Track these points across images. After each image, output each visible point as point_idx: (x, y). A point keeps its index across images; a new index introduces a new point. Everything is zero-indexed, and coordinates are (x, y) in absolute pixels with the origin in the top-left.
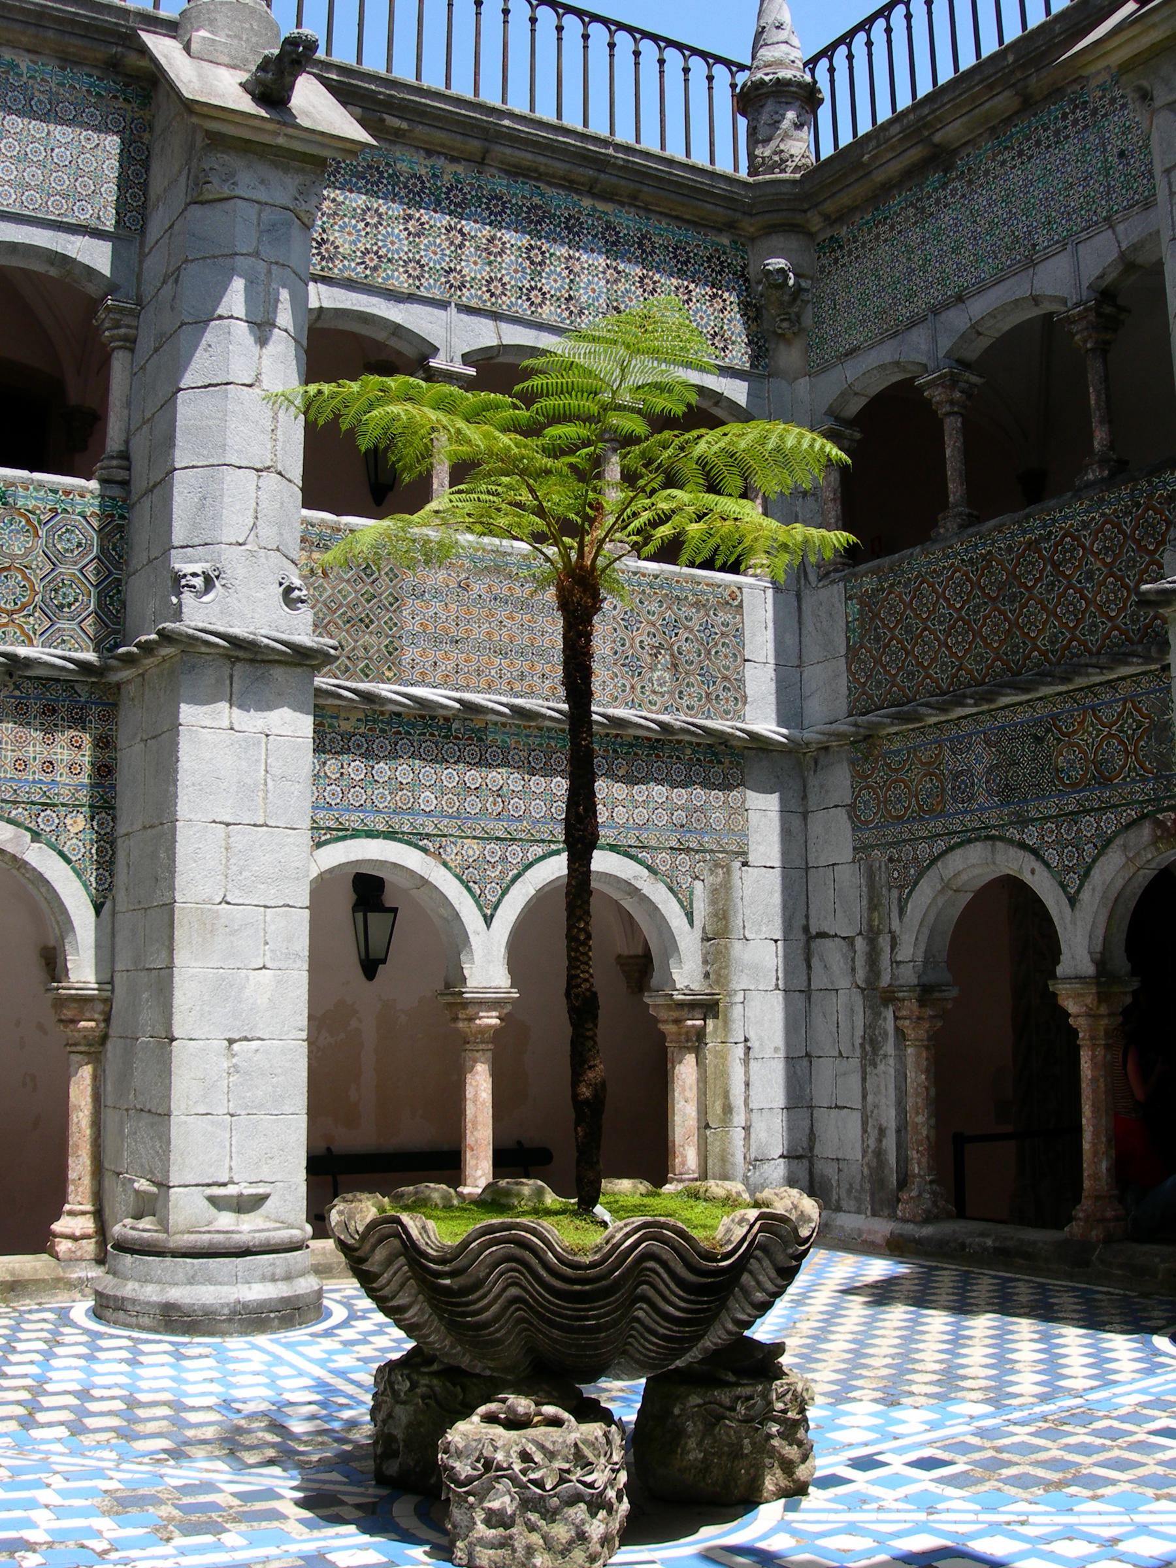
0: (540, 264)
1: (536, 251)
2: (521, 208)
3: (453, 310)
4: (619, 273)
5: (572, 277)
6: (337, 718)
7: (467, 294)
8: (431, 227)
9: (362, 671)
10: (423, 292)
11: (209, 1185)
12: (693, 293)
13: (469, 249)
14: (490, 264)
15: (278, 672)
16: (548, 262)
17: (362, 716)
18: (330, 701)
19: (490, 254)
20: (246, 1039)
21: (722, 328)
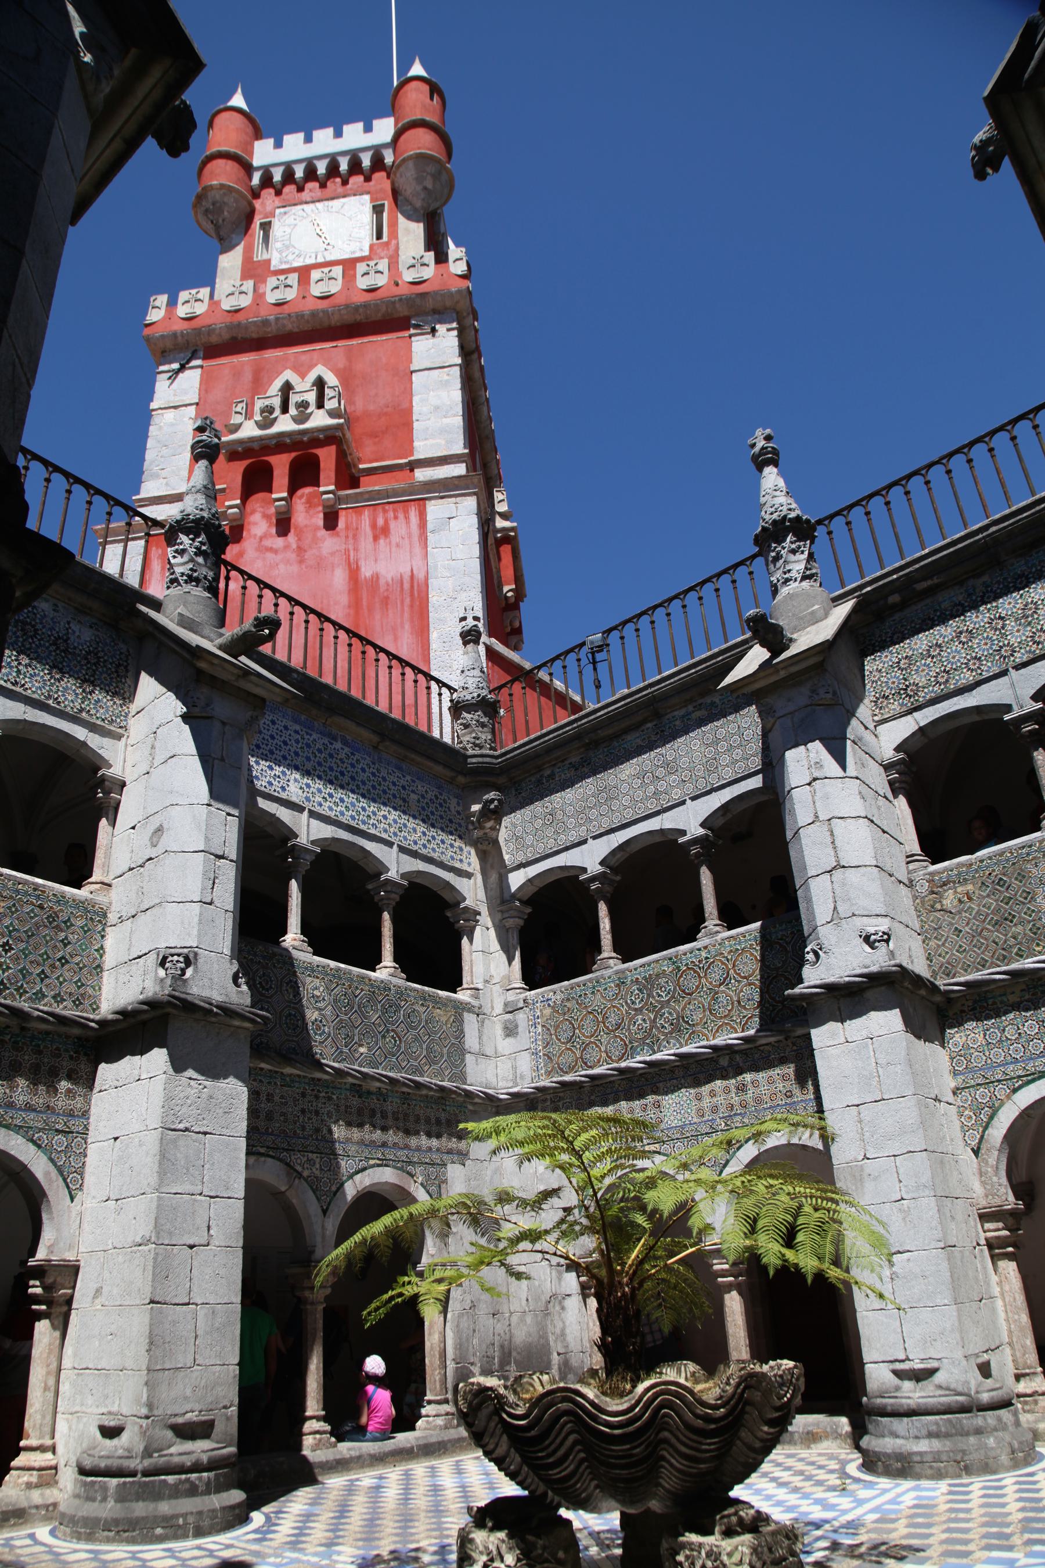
3: (1012, 672)
6: (1005, 995)
7: (1019, 655)
9: (1017, 954)
10: (986, 675)
11: (891, 1362)
13: (1011, 624)
14: (1029, 624)
15: (869, 994)
17: (1024, 987)
18: (992, 987)
19: (1027, 617)
20: (899, 1252)
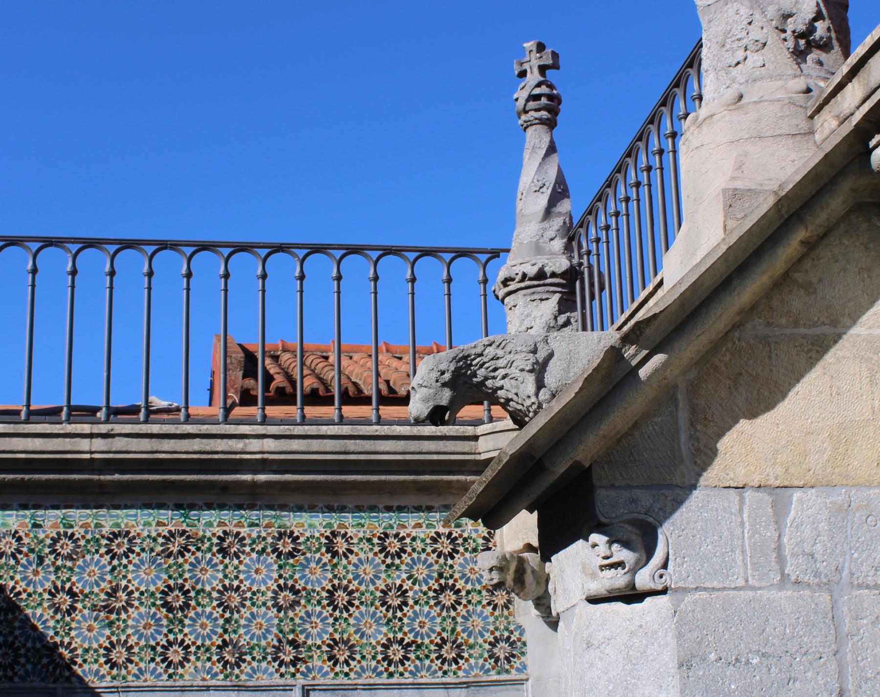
0: (182, 608)
1: (177, 592)
2: (155, 540)
4: (296, 592)
5: (227, 615)
8: (30, 595)
12: (410, 594)
16: (193, 603)
21: (453, 630)
